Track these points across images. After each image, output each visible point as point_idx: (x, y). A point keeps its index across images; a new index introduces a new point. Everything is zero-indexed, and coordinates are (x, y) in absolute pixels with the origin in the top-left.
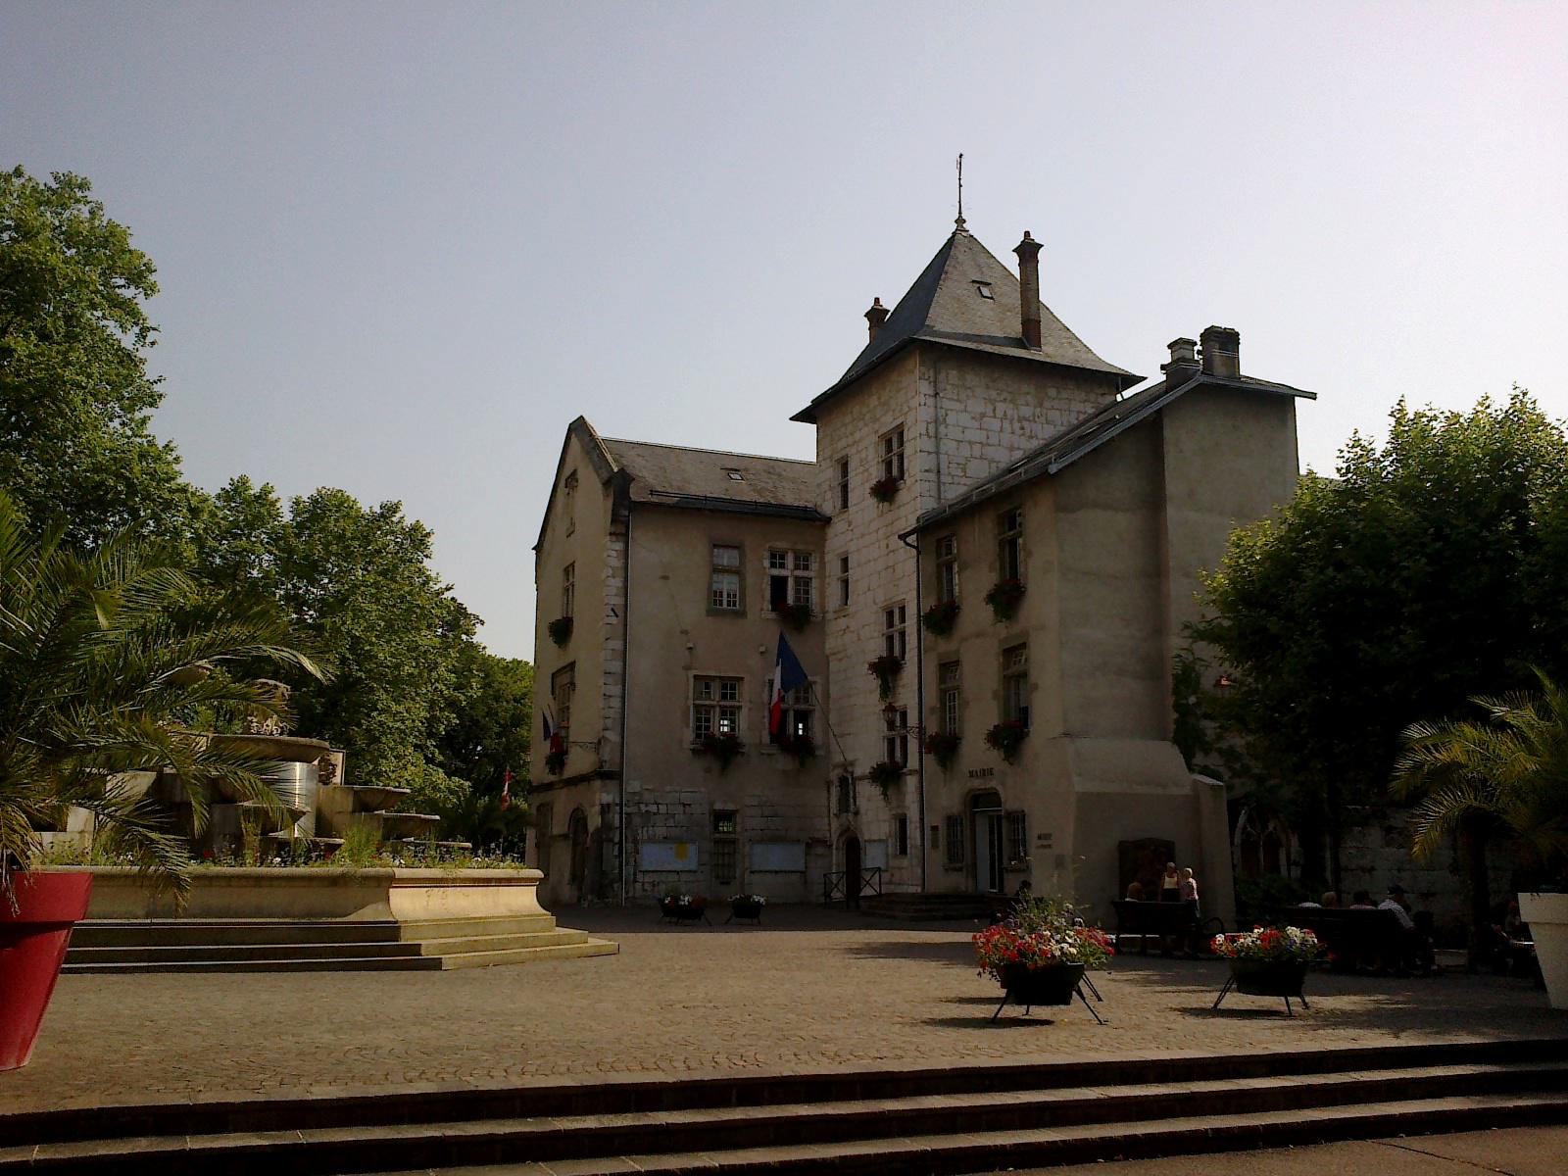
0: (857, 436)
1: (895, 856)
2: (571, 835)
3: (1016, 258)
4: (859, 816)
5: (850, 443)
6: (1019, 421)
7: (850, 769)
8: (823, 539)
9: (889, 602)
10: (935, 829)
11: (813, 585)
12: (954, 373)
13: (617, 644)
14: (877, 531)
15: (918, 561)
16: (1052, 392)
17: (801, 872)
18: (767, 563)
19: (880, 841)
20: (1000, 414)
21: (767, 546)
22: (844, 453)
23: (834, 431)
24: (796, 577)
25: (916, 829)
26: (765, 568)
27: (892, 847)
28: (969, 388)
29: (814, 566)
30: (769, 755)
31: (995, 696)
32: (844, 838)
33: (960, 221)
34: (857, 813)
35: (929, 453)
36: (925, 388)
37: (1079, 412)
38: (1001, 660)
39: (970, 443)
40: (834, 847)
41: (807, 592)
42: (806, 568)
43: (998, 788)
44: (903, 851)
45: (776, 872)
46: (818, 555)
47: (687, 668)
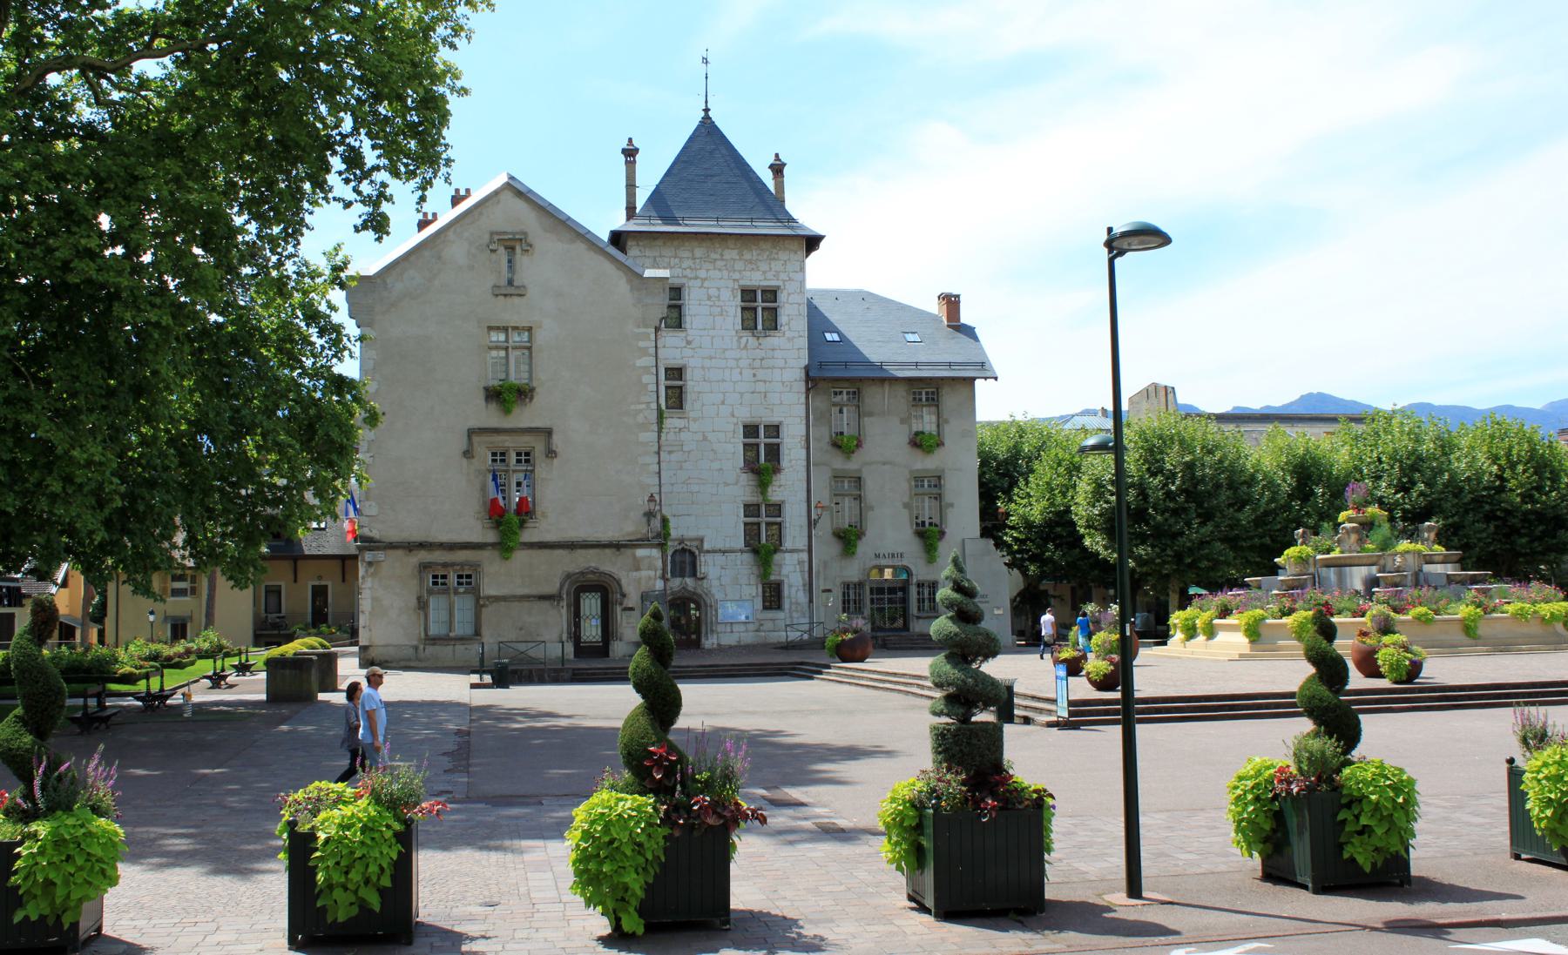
0: (702, 274)
2: (565, 596)
9: (755, 420)
15: (807, 398)
23: (661, 256)
33: (707, 110)
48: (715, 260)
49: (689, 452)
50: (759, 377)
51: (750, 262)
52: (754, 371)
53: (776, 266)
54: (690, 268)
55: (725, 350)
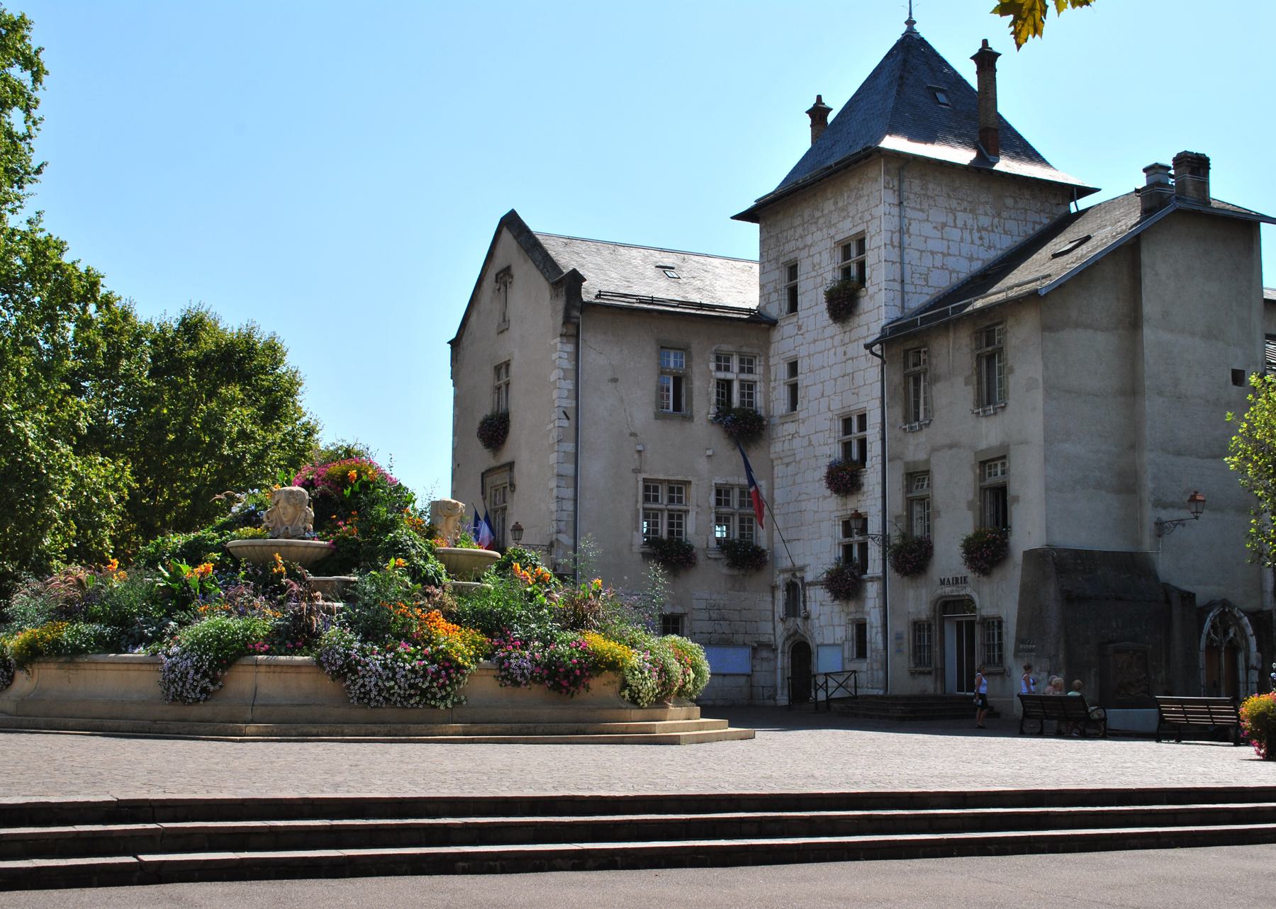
0: (809, 240)
1: (851, 660)
3: (973, 66)
4: (809, 621)
5: (801, 247)
6: (979, 231)
7: (798, 574)
8: (767, 343)
9: (846, 410)
10: (899, 637)
11: (758, 389)
12: (917, 182)
13: (570, 447)
14: (832, 338)
15: (882, 370)
16: (1009, 202)
17: (749, 676)
18: (712, 366)
19: (834, 645)
20: (960, 223)
21: (713, 350)
22: (792, 256)
24: (741, 381)
25: (877, 633)
26: (711, 371)
27: (849, 650)
28: (932, 197)
29: (759, 369)
30: (716, 559)
31: (970, 505)
32: (790, 642)
33: (910, 23)
34: (807, 618)
35: (893, 263)
36: (891, 197)
37: (1035, 223)
38: (978, 471)
39: (932, 253)
40: (779, 651)
41: (750, 395)
42: (750, 371)
43: (972, 594)
44: (861, 652)
45: (724, 675)
46: (763, 358)
47: (637, 471)
48: (818, 218)
49: (799, 462)
50: (849, 355)
51: (843, 209)
52: (844, 348)
53: (862, 205)
54: (801, 237)
55: (825, 327)
